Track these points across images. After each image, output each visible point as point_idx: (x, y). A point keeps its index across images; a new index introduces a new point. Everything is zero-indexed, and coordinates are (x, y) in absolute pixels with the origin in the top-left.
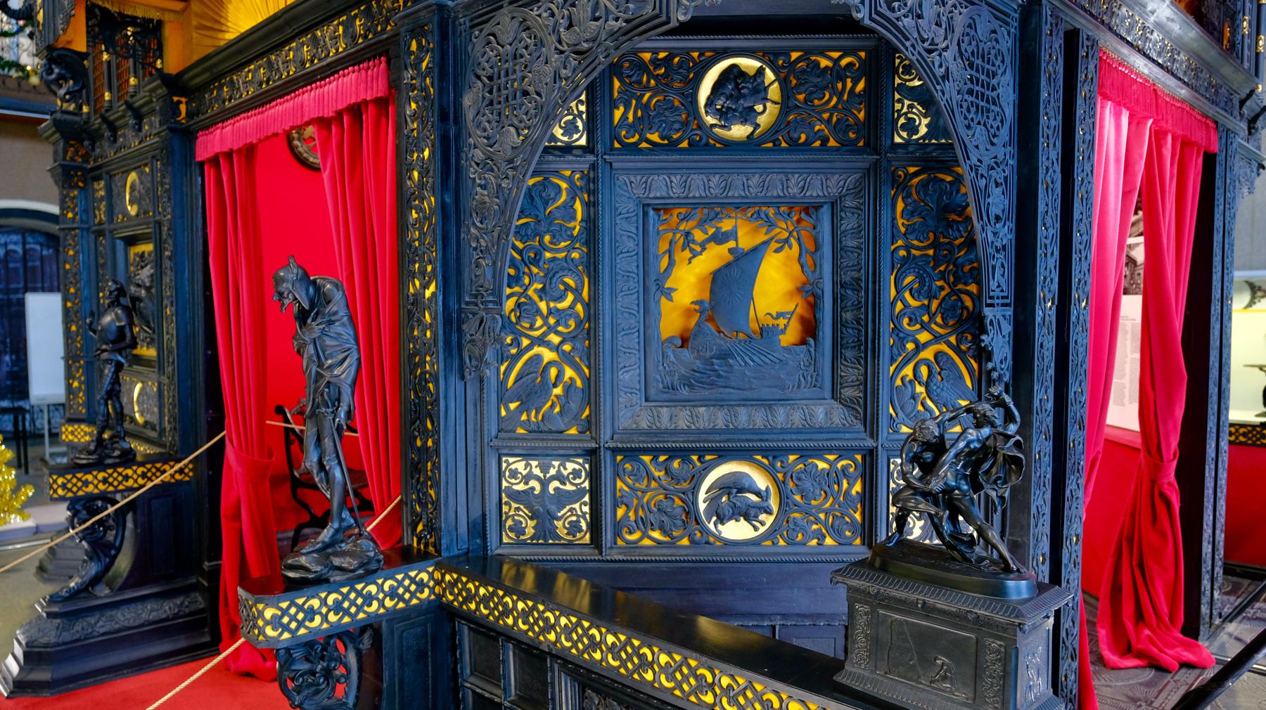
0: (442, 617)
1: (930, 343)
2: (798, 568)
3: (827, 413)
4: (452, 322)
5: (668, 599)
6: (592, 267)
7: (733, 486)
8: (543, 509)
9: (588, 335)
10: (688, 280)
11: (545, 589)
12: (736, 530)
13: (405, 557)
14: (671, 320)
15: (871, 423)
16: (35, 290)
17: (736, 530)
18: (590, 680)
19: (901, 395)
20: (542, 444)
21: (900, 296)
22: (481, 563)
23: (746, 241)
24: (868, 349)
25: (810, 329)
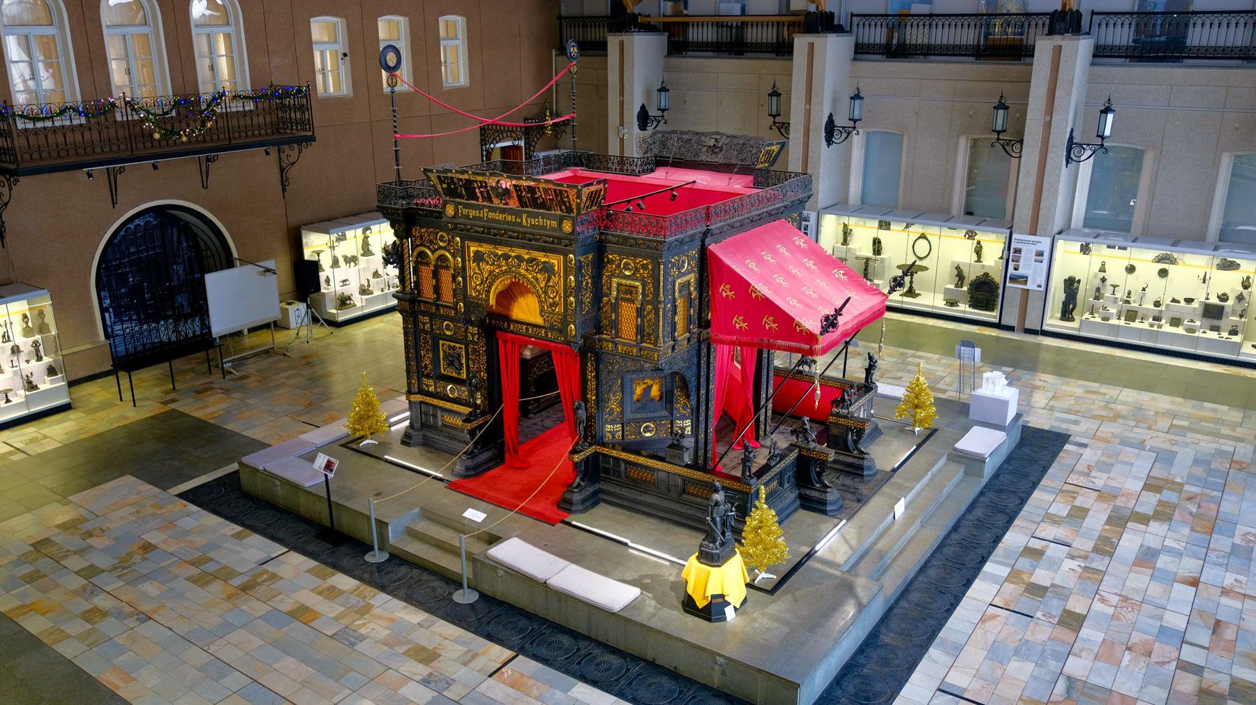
0: (596, 454)
1: (682, 400)
2: (661, 440)
3: (664, 413)
4: (597, 402)
5: (636, 447)
6: (622, 391)
7: (647, 427)
8: (613, 434)
9: (621, 404)
10: (639, 391)
11: (614, 448)
12: (648, 435)
13: (591, 445)
14: (635, 397)
15: (672, 414)
16: (210, 271)
17: (648, 435)
18: (627, 462)
19: (678, 410)
20: (613, 422)
21: (677, 392)
22: (604, 445)
23: (650, 382)
24: (671, 402)
25: (661, 398)
